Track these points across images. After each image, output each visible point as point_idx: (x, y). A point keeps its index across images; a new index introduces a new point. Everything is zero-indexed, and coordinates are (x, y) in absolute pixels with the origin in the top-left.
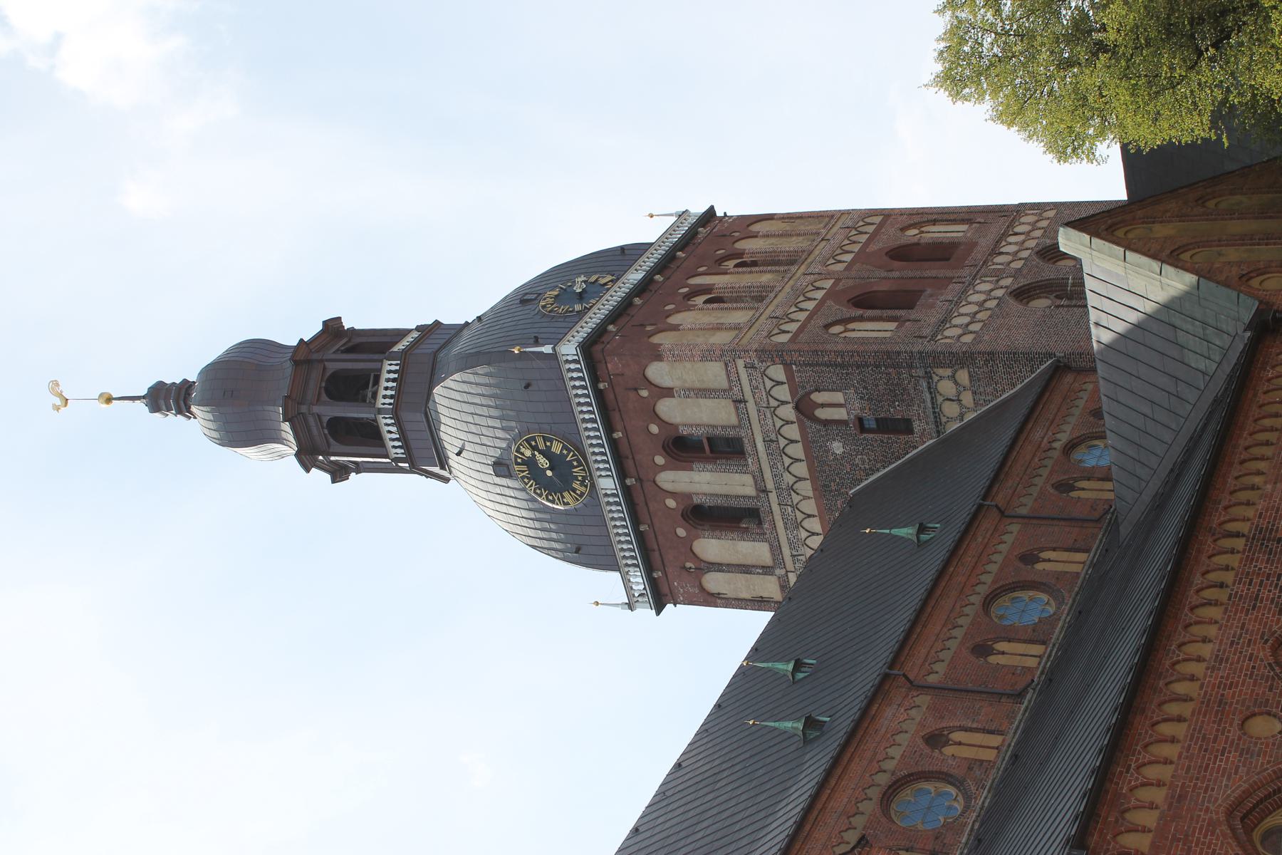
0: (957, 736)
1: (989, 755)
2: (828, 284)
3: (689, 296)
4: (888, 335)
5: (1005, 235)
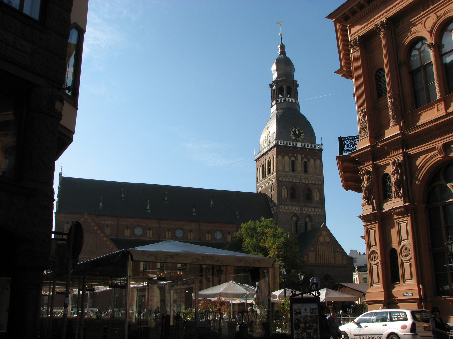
0: (192, 234)
1: (189, 238)
2: (298, 181)
3: (294, 156)
4: (283, 196)
5: (314, 207)
